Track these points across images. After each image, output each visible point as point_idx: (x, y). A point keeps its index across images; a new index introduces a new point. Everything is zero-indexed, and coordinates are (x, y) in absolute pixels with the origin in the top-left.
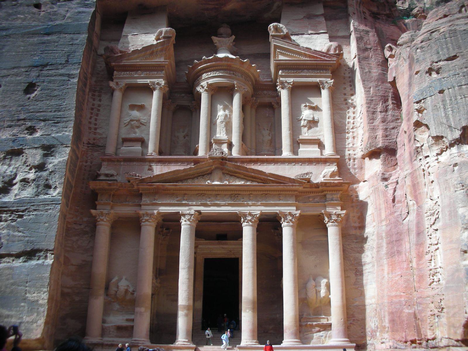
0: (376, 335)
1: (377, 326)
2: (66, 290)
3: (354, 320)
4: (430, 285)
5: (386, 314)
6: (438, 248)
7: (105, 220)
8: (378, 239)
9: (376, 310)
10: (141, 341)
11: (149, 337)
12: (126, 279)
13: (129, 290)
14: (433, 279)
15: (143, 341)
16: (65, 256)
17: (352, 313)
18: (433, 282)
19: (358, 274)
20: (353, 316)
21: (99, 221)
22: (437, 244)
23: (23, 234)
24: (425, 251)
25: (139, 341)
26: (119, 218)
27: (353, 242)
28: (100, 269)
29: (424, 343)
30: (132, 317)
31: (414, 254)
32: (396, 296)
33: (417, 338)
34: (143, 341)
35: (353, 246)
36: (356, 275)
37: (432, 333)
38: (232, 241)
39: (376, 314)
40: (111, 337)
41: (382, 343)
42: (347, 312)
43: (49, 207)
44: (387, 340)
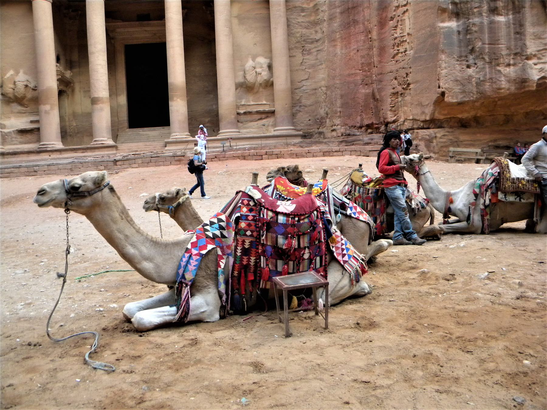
0: (326, 122)
1: (327, 112)
3: (300, 106)
4: (393, 57)
5: (339, 96)
6: (407, 10)
8: (330, 9)
9: (326, 94)
10: (50, 144)
12: (25, 73)
13: (30, 85)
14: (398, 50)
15: (53, 144)
17: (298, 98)
18: (397, 54)
19: (305, 53)
20: (299, 101)
22: (405, 5)
24: (390, 15)
25: (47, 145)
27: (300, 15)
29: (383, 128)
31: (375, 20)
32: (349, 75)
33: (374, 122)
35: (299, 21)
36: (303, 54)
37: (393, 115)
38: (155, 22)
39: (326, 99)
40: (14, 144)
41: (333, 130)
42: (292, 98)
44: (339, 127)
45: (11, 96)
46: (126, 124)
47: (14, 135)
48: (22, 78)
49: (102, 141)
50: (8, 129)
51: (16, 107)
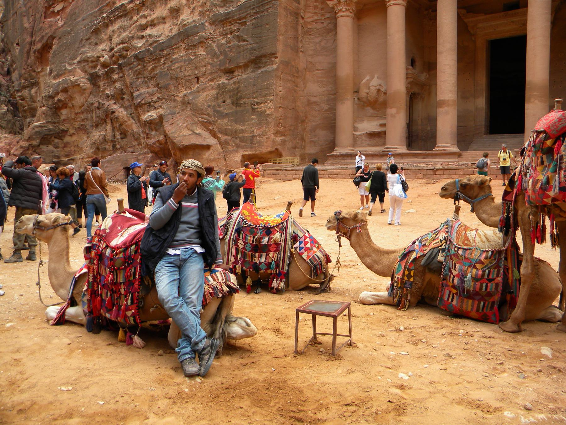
2: (313, 99)
7: (344, 10)
10: (393, 148)
11: (405, 143)
12: (378, 78)
15: (396, 148)
16: (307, 61)
21: (338, 13)
23: (246, 43)
25: (391, 148)
26: (365, 5)
28: (345, 69)
30: (382, 122)
34: (396, 148)
40: (364, 147)
43: (269, 6)
45: (364, 100)
46: (483, 130)
47: (364, 138)
48: (375, 83)
49: (444, 147)
50: (360, 131)
51: (370, 110)
